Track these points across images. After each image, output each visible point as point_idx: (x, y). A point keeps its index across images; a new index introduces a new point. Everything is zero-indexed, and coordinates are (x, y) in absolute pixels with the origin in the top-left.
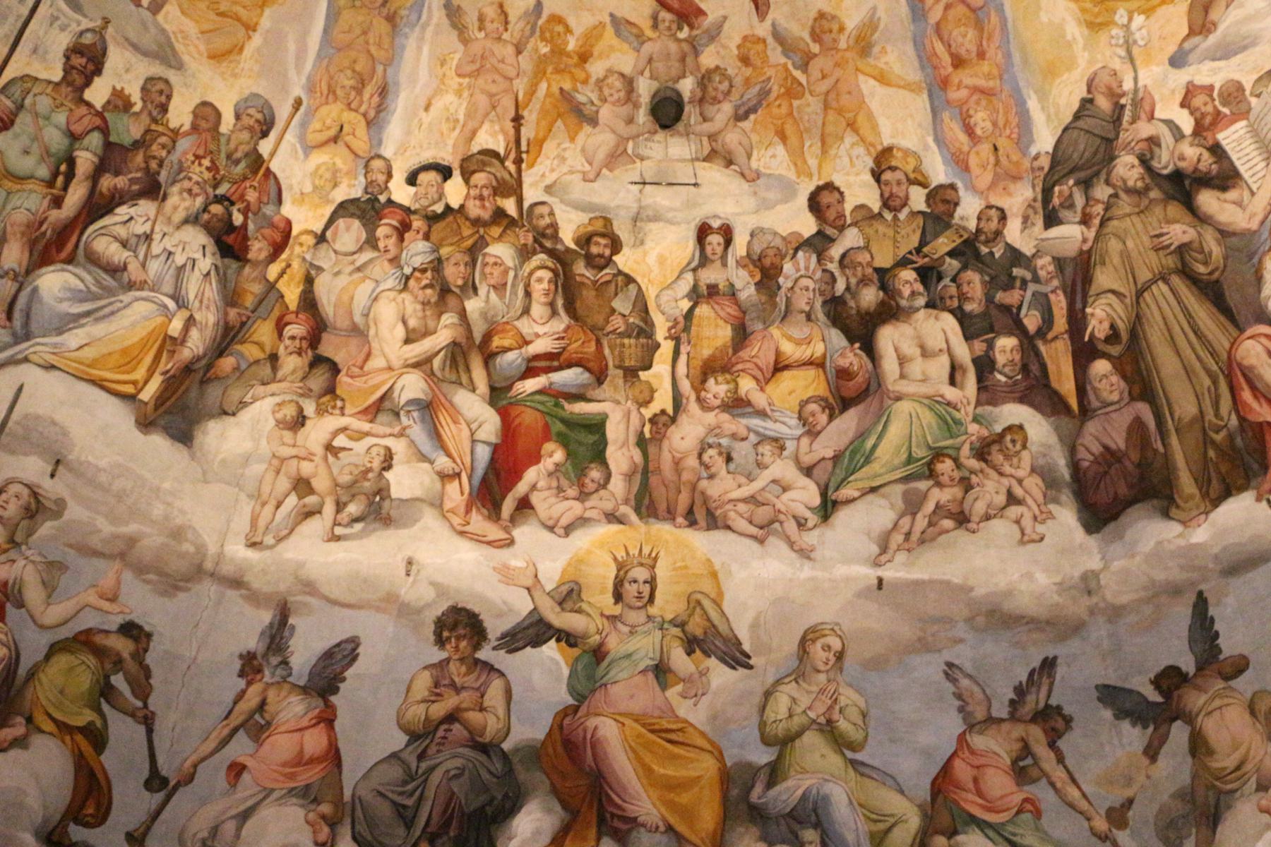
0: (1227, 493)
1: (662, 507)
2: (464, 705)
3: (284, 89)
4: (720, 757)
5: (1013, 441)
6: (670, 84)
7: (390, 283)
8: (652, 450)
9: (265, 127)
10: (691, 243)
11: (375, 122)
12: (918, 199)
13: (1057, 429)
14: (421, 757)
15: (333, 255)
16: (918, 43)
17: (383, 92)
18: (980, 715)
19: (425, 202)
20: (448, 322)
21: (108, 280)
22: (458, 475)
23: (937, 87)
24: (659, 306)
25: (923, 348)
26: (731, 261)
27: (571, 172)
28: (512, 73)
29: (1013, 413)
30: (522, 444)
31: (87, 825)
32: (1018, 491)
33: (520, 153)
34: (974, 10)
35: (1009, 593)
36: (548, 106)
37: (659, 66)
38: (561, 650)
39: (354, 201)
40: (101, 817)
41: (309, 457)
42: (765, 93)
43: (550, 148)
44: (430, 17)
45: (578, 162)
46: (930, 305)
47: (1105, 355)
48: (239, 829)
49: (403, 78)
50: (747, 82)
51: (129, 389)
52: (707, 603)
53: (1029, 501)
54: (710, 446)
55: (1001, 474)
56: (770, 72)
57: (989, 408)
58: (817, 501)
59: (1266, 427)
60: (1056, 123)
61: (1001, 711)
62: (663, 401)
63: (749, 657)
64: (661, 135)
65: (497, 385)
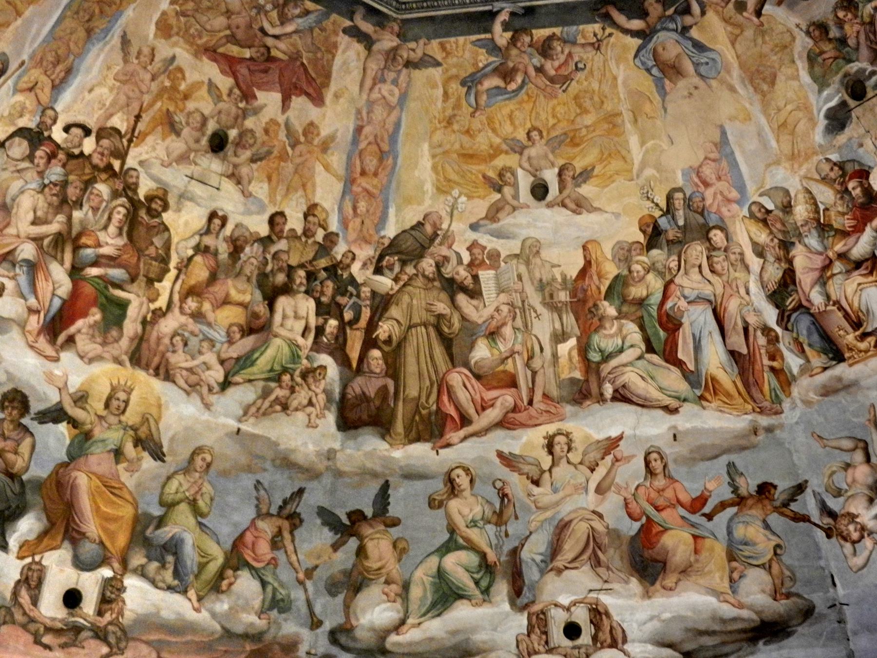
0: (418, 439)
1: (144, 362)
2: (7, 449)
3: (19, 53)
4: (136, 508)
5: (320, 374)
6: (225, 129)
7: (34, 185)
8: (148, 328)
10: (204, 220)
11: (57, 87)
12: (320, 235)
13: (341, 373)
15: (5, 157)
16: (349, 158)
17: (69, 71)
18: (264, 511)
19: (69, 145)
20: (61, 220)
23: (349, 182)
24: (176, 249)
25: (295, 312)
26: (221, 236)
27: (156, 158)
28: (144, 89)
29: (325, 359)
30: (80, 303)
32: (314, 400)
33: (133, 137)
35: (293, 451)
36: (158, 117)
37: (224, 117)
38: (68, 429)
39: (29, 130)
42: (269, 153)
43: (150, 140)
44: (110, 40)
45: (163, 155)
46: (307, 292)
47: (379, 348)
49: (83, 68)
53: (318, 407)
54: (179, 335)
55: (310, 389)
56: (276, 143)
57: (315, 354)
59: (449, 419)
60: (400, 226)
61: (274, 510)
62: (162, 302)
63: (164, 455)
64: (209, 155)
65: (77, 266)
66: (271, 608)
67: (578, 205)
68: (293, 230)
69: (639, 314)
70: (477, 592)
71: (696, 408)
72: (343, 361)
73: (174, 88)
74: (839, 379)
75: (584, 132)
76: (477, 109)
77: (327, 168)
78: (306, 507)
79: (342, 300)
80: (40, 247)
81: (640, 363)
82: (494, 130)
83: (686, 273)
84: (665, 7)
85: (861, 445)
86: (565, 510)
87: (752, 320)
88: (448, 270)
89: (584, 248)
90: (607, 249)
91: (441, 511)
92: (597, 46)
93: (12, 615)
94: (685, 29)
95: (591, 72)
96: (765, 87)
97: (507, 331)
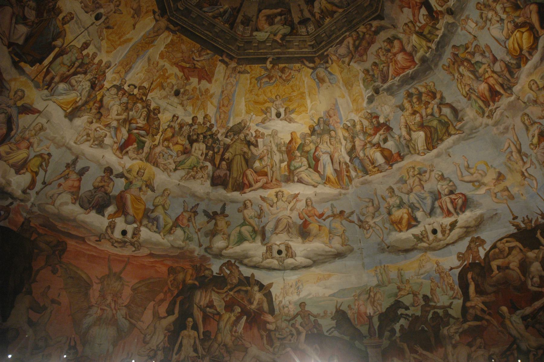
1: (150, 161)
4: (145, 206)
8: (152, 150)
9: (108, 67)
10: (171, 117)
11: (127, 72)
13: (213, 168)
14: (95, 192)
17: (131, 68)
18: (186, 210)
21: (71, 88)
22: (117, 143)
29: (208, 164)
31: (30, 190)
32: (204, 176)
33: (150, 90)
34: (230, 99)
40: (33, 188)
41: (91, 130)
42: (193, 97)
43: (155, 91)
46: (203, 142)
47: (225, 161)
48: (58, 196)
50: (191, 94)
51: (66, 109)
52: (151, 179)
58: (174, 168)
61: (189, 210)
62: (156, 142)
64: (174, 97)
66: (186, 240)
67: (290, 120)
68: (199, 122)
69: (307, 156)
70: (251, 239)
71: (323, 186)
72: (214, 164)
73: (164, 75)
74: (366, 180)
75: (293, 97)
76: (260, 88)
77: (212, 103)
78: (200, 210)
79: (214, 145)
80: (119, 123)
81: (306, 171)
82: (265, 95)
83: (322, 144)
84: (321, 61)
85: (371, 200)
86: (280, 215)
87: (342, 160)
88: (248, 138)
89: (291, 134)
90: (298, 135)
91: (242, 213)
92: (299, 71)
93: (105, 237)
94: (326, 68)
95: (297, 79)
96: (350, 88)
97: (266, 158)
